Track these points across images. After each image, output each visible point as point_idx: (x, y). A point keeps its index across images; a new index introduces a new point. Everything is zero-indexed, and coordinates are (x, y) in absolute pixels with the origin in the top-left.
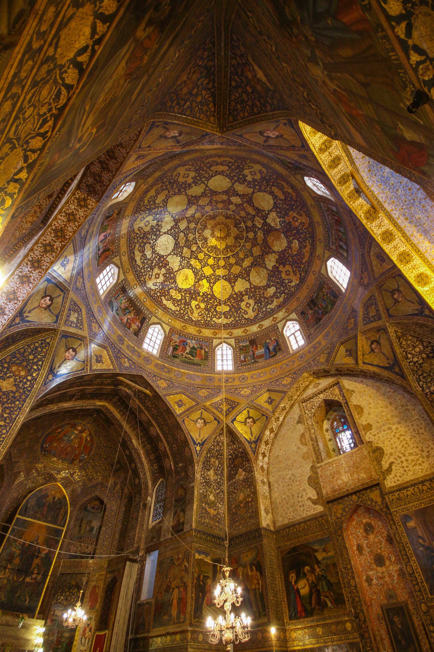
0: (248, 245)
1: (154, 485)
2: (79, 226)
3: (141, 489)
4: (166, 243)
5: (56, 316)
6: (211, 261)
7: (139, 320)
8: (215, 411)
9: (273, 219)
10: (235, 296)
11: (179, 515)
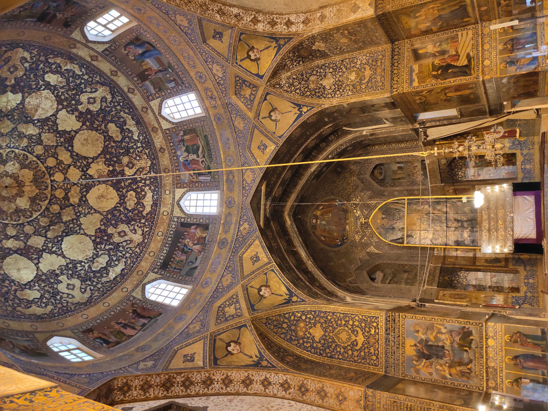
1: (349, 132)
2: (149, 375)
3: (357, 142)
5: (240, 330)
6: (58, 177)
7: (188, 230)
8: (256, 103)
10: (88, 124)
11: (377, 108)
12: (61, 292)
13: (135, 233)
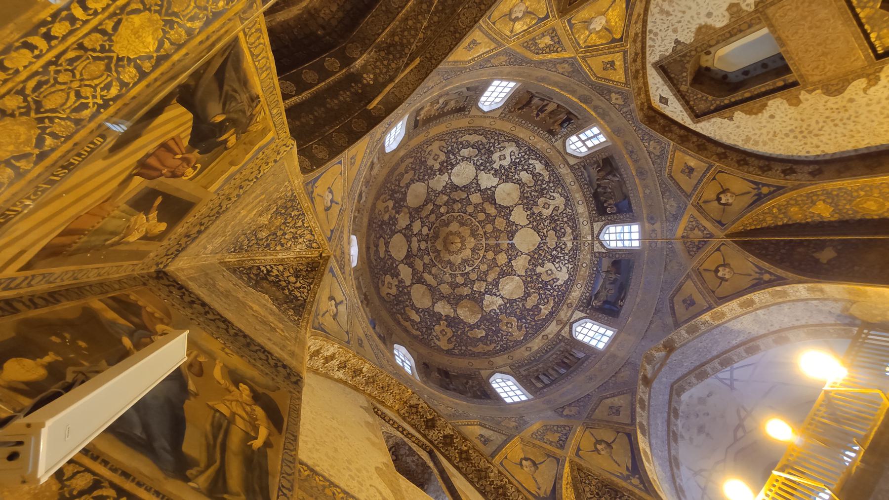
0: (447, 278)
4: (465, 176)
6: (425, 231)
9: (493, 302)
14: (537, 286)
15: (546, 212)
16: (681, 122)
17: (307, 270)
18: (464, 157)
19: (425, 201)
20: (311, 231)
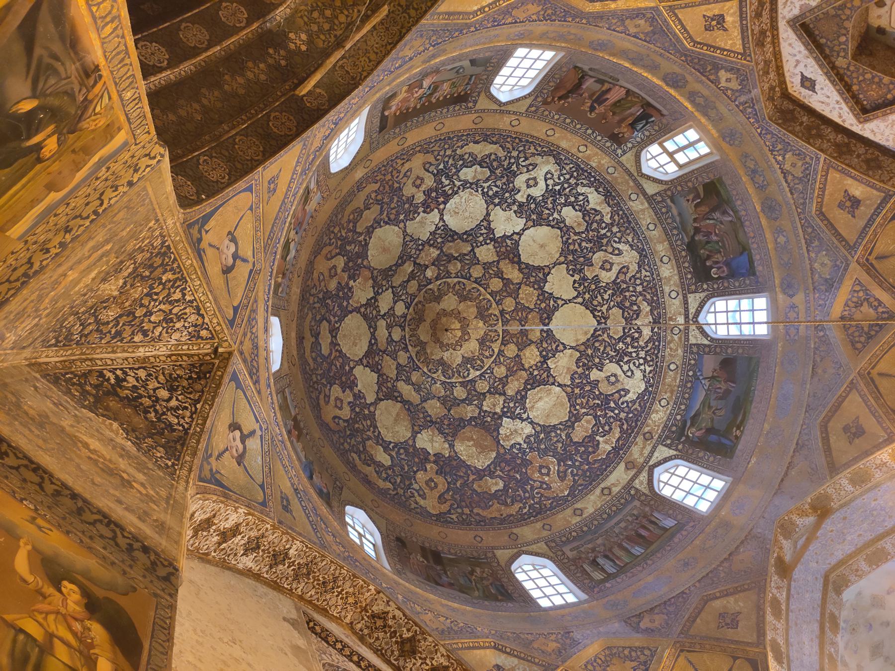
4: (467, 214)
6: (400, 309)
9: (516, 431)
10: (347, 368)
12: (547, 188)
13: (410, 170)
14: (591, 403)
15: (607, 277)
16: (838, 120)
17: (190, 378)
18: (466, 182)
19: (400, 257)
20: (198, 309)
